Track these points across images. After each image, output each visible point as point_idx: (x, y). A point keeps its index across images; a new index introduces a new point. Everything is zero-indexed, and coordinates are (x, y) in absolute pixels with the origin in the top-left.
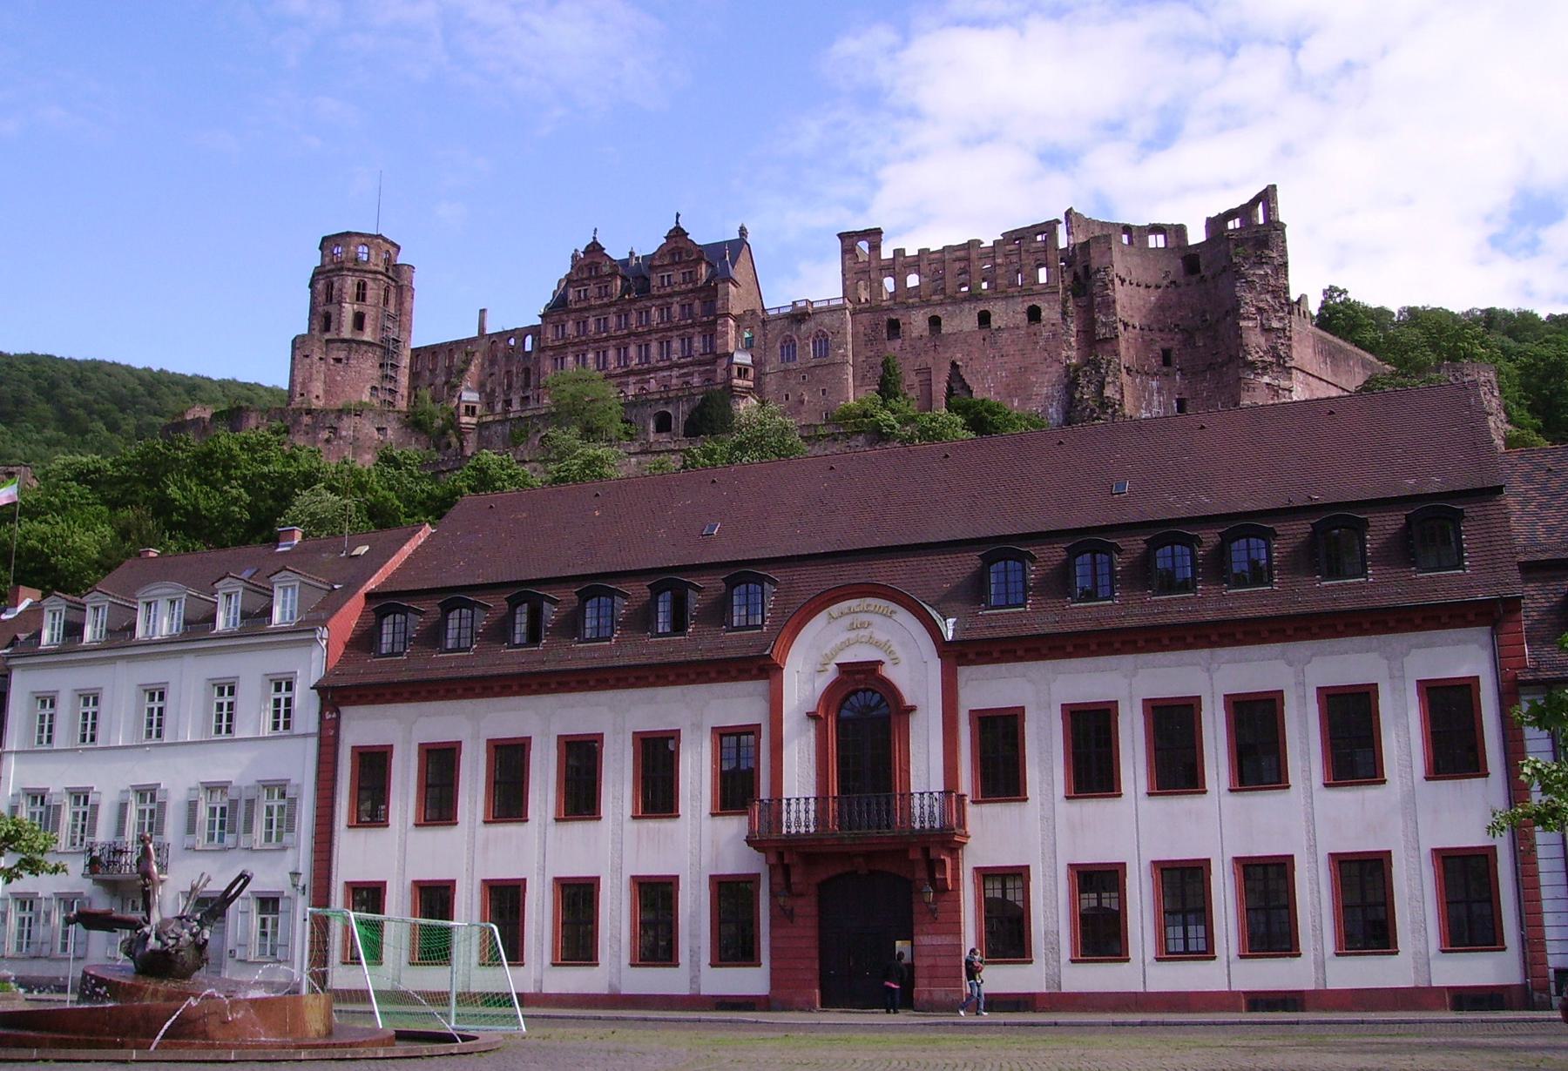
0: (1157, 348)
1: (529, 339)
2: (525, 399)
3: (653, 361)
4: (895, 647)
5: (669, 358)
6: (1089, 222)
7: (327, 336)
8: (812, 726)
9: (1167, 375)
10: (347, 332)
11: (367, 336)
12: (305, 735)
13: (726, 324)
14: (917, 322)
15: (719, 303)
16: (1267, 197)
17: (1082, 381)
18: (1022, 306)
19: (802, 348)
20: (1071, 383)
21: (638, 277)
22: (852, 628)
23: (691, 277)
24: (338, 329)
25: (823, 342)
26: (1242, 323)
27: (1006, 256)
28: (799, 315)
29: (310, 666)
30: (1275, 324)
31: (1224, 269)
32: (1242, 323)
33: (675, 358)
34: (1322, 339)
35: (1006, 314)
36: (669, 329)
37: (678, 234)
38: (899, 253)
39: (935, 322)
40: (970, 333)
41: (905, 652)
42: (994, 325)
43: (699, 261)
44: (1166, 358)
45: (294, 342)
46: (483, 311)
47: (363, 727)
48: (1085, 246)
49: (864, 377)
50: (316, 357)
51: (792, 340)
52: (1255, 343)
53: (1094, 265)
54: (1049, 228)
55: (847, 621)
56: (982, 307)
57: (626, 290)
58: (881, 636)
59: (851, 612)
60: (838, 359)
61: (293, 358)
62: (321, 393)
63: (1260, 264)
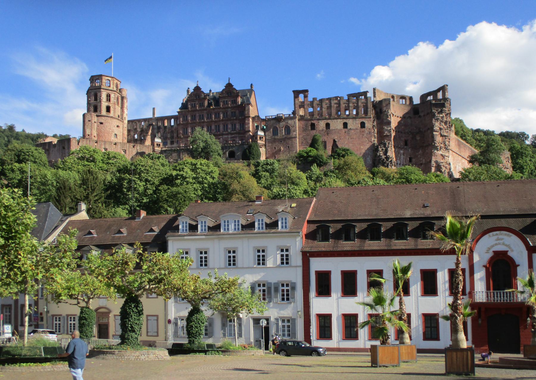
0: (403, 139)
1: (172, 120)
2: (172, 143)
3: (221, 131)
4: (512, 246)
5: (227, 131)
6: (381, 92)
7: (98, 114)
8: (484, 269)
9: (406, 149)
10: (104, 112)
11: (112, 114)
12: (296, 267)
13: (249, 120)
14: (322, 125)
15: (246, 112)
16: (443, 89)
17: (380, 149)
18: (359, 121)
19: (280, 131)
20: (374, 149)
21: (216, 100)
22: (498, 239)
23: (235, 101)
24: (100, 111)
25: (288, 129)
26: (434, 133)
27: (353, 103)
28: (278, 119)
29: (297, 244)
30: (445, 134)
31: (428, 114)
32: (434, 133)
33: (229, 131)
34: (458, 141)
35: (351, 124)
36: (227, 120)
37: (229, 86)
38: (314, 99)
39: (328, 125)
40: (340, 130)
41: (516, 249)
42: (349, 127)
43: (238, 96)
44: (406, 144)
45: (84, 115)
46: (154, 109)
47: (318, 265)
48: (381, 102)
49: (302, 143)
50: (93, 122)
51: (277, 128)
52: (438, 139)
53: (384, 109)
54: (365, 93)
55: (496, 237)
56: (345, 121)
57: (210, 104)
58: (506, 243)
59: (497, 234)
60: (294, 136)
61: (84, 121)
62: (96, 135)
63: (441, 112)
